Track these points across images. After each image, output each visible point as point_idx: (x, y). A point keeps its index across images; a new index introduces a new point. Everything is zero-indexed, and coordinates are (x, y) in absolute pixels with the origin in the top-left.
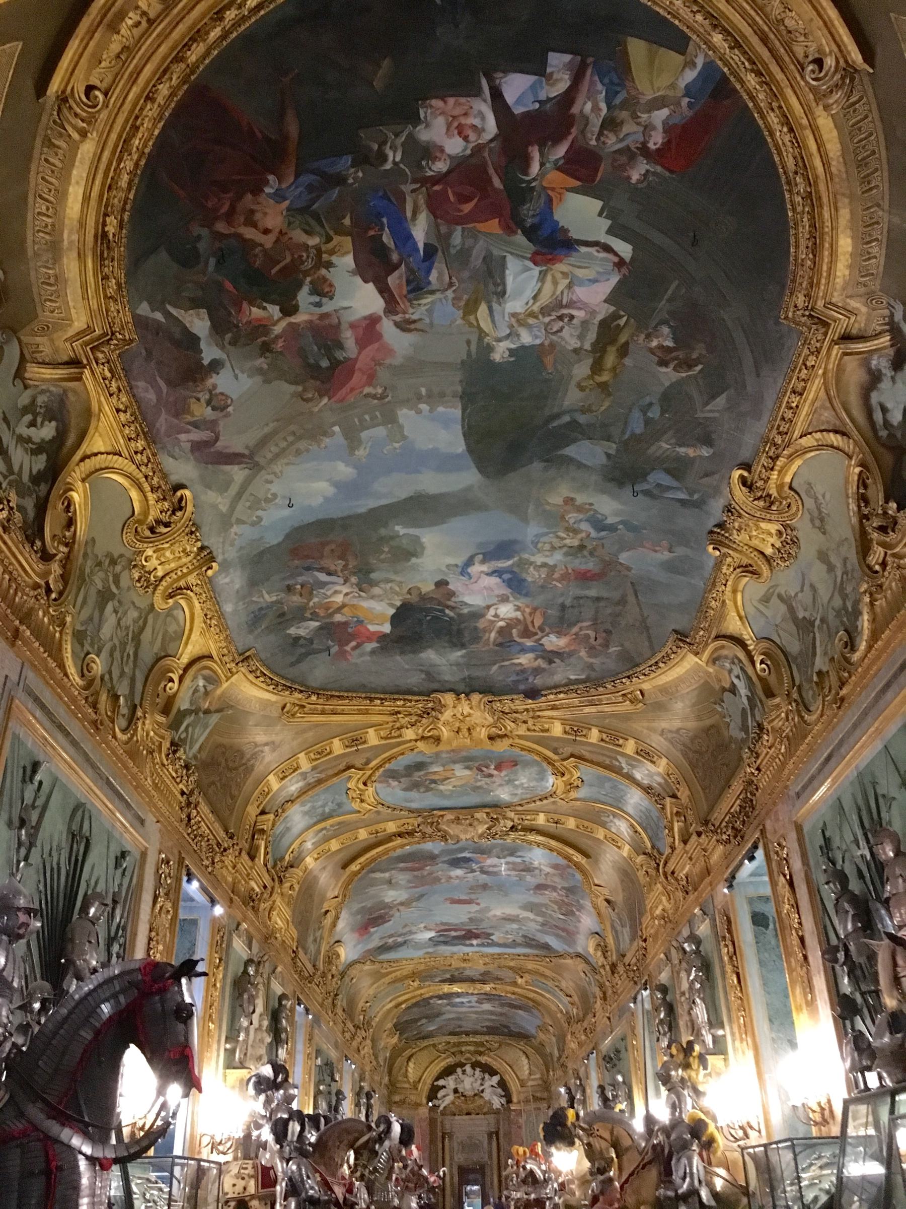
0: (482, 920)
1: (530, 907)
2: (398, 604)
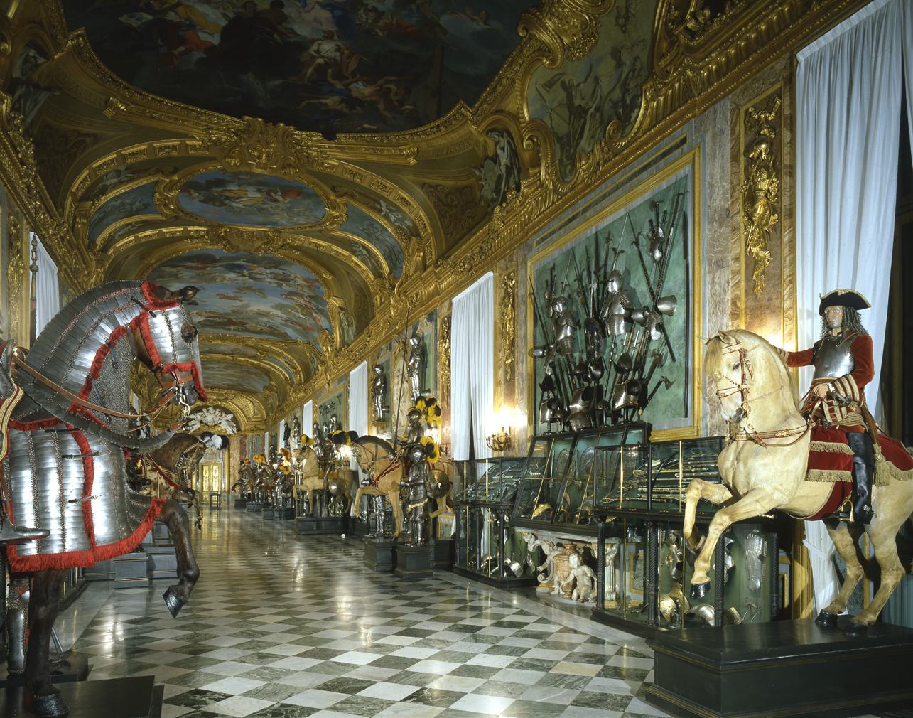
1: (280, 307)
2: (231, 15)
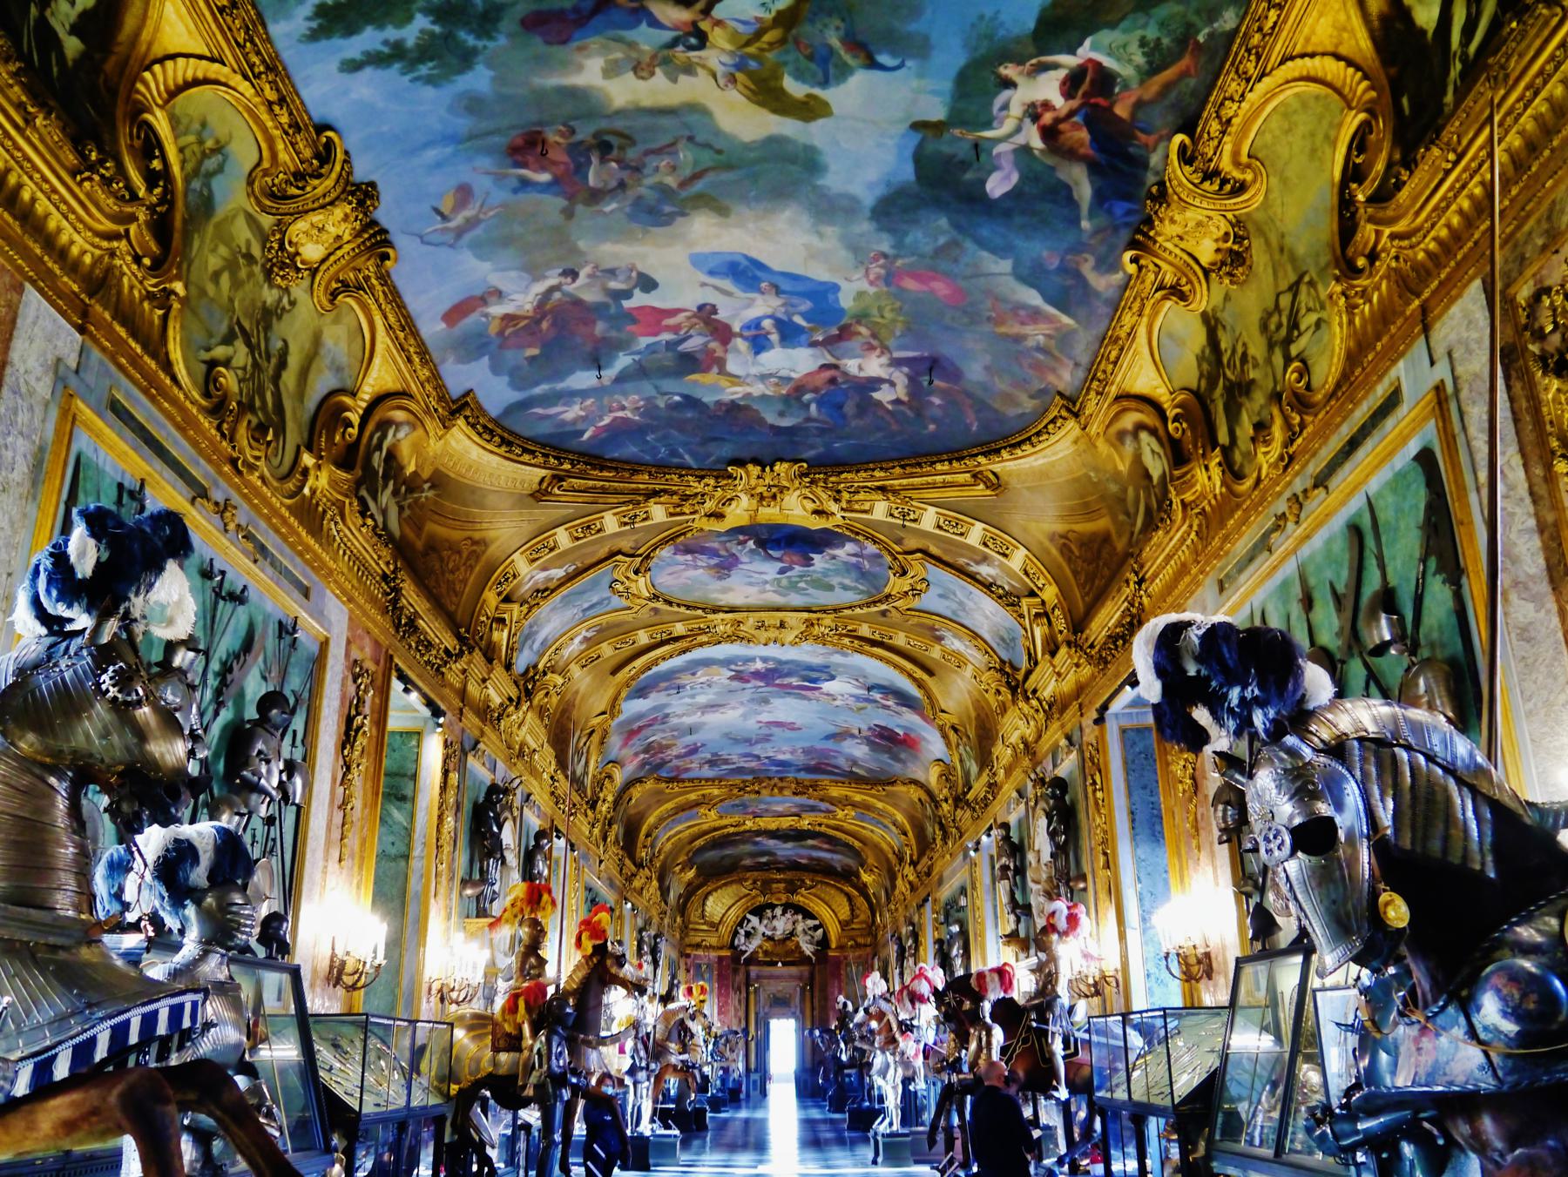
0: (752, 700)
1: (691, 730)
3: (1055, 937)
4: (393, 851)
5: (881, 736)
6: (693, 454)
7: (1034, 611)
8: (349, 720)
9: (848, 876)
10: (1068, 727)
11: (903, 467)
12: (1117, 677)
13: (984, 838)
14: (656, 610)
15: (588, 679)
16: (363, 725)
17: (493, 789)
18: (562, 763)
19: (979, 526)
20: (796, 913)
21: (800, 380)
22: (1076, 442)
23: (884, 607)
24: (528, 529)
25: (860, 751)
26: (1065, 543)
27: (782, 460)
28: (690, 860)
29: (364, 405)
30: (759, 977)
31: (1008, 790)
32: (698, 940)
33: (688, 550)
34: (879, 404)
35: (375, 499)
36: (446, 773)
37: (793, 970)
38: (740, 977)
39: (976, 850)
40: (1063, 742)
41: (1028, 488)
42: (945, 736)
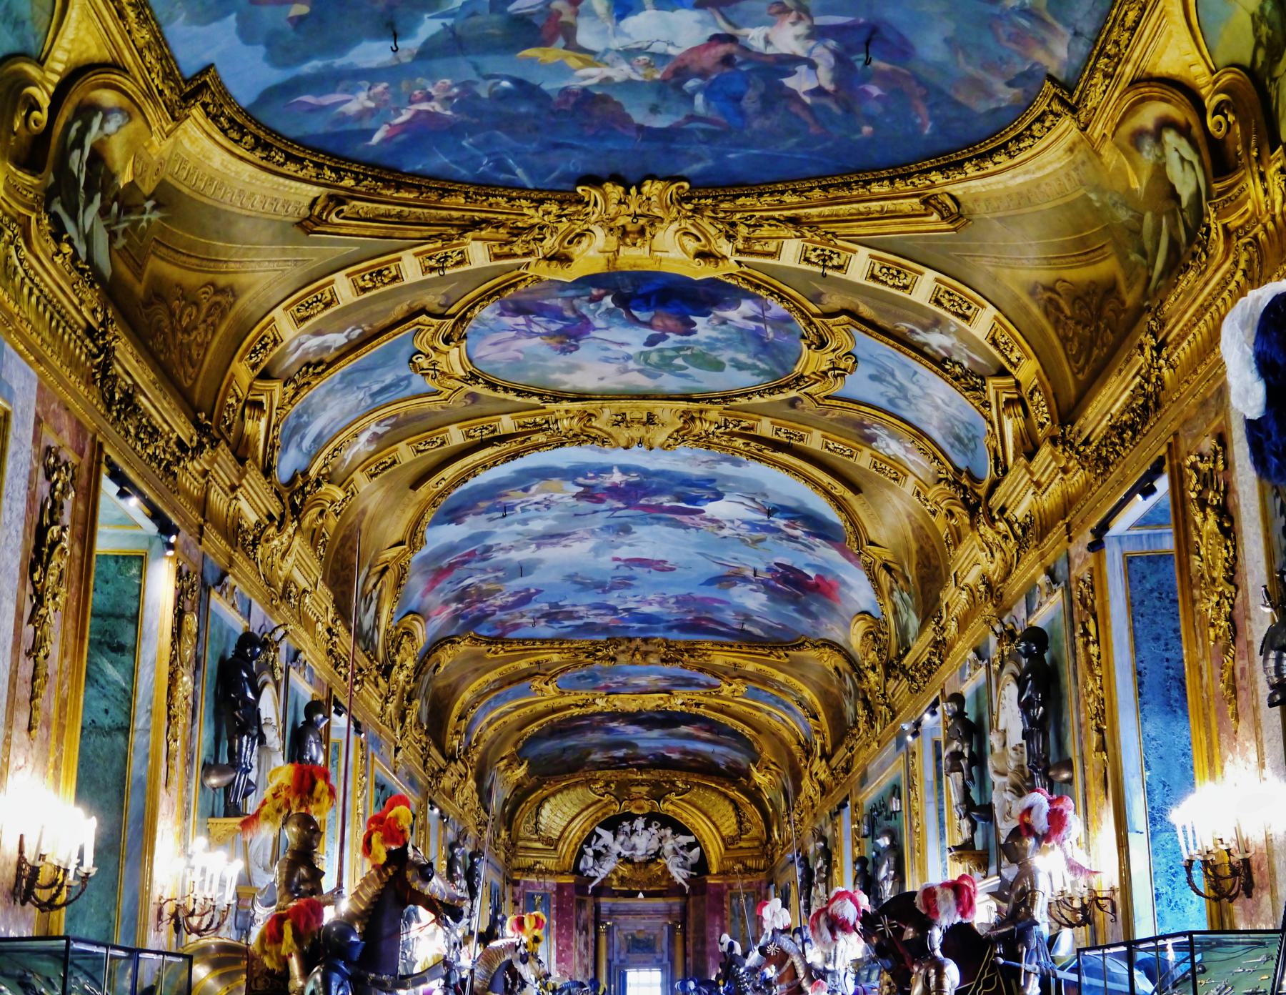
0: (607, 528)
1: (522, 570)
3: (1031, 842)
4: (106, 721)
5: (786, 581)
6: (529, 170)
7: (1004, 397)
8: (41, 532)
9: (735, 776)
10: (1049, 560)
11: (825, 188)
12: (1121, 484)
13: (927, 717)
14: (474, 397)
15: (379, 494)
16: (61, 539)
17: (248, 639)
18: (343, 610)
19: (930, 275)
20: (664, 826)
21: (681, 58)
22: (1071, 150)
23: (793, 394)
24: (296, 273)
25: (753, 600)
26: (1049, 297)
27: (653, 178)
28: (519, 752)
29: (56, 79)
30: (612, 912)
31: (963, 650)
32: (530, 861)
33: (519, 309)
34: (793, 95)
35: (74, 218)
36: (179, 615)
37: (659, 903)
38: (587, 913)
39: (915, 734)
40: (1042, 579)
41: (1000, 219)
42: (874, 579)
